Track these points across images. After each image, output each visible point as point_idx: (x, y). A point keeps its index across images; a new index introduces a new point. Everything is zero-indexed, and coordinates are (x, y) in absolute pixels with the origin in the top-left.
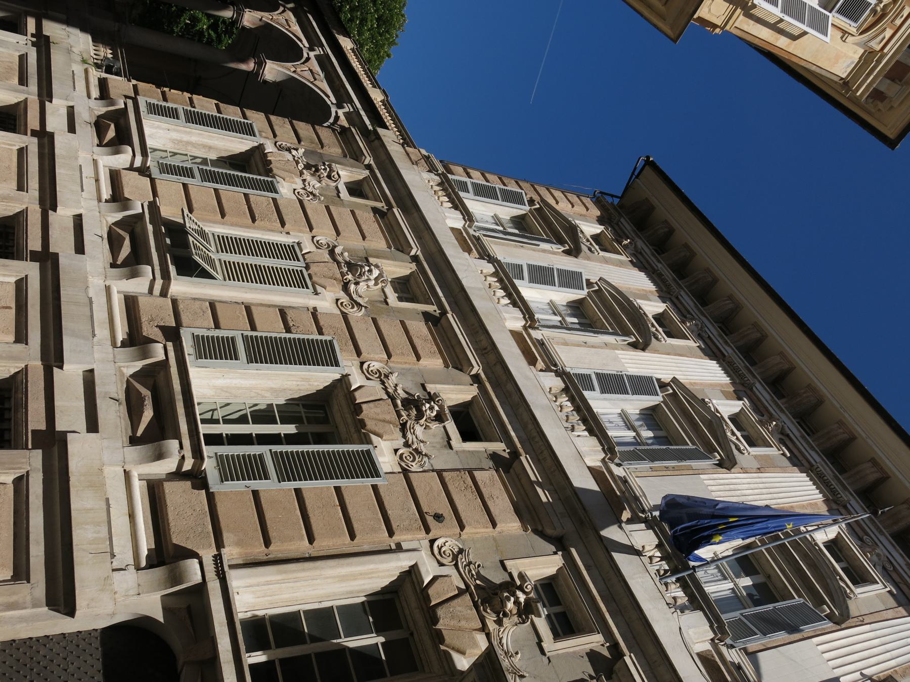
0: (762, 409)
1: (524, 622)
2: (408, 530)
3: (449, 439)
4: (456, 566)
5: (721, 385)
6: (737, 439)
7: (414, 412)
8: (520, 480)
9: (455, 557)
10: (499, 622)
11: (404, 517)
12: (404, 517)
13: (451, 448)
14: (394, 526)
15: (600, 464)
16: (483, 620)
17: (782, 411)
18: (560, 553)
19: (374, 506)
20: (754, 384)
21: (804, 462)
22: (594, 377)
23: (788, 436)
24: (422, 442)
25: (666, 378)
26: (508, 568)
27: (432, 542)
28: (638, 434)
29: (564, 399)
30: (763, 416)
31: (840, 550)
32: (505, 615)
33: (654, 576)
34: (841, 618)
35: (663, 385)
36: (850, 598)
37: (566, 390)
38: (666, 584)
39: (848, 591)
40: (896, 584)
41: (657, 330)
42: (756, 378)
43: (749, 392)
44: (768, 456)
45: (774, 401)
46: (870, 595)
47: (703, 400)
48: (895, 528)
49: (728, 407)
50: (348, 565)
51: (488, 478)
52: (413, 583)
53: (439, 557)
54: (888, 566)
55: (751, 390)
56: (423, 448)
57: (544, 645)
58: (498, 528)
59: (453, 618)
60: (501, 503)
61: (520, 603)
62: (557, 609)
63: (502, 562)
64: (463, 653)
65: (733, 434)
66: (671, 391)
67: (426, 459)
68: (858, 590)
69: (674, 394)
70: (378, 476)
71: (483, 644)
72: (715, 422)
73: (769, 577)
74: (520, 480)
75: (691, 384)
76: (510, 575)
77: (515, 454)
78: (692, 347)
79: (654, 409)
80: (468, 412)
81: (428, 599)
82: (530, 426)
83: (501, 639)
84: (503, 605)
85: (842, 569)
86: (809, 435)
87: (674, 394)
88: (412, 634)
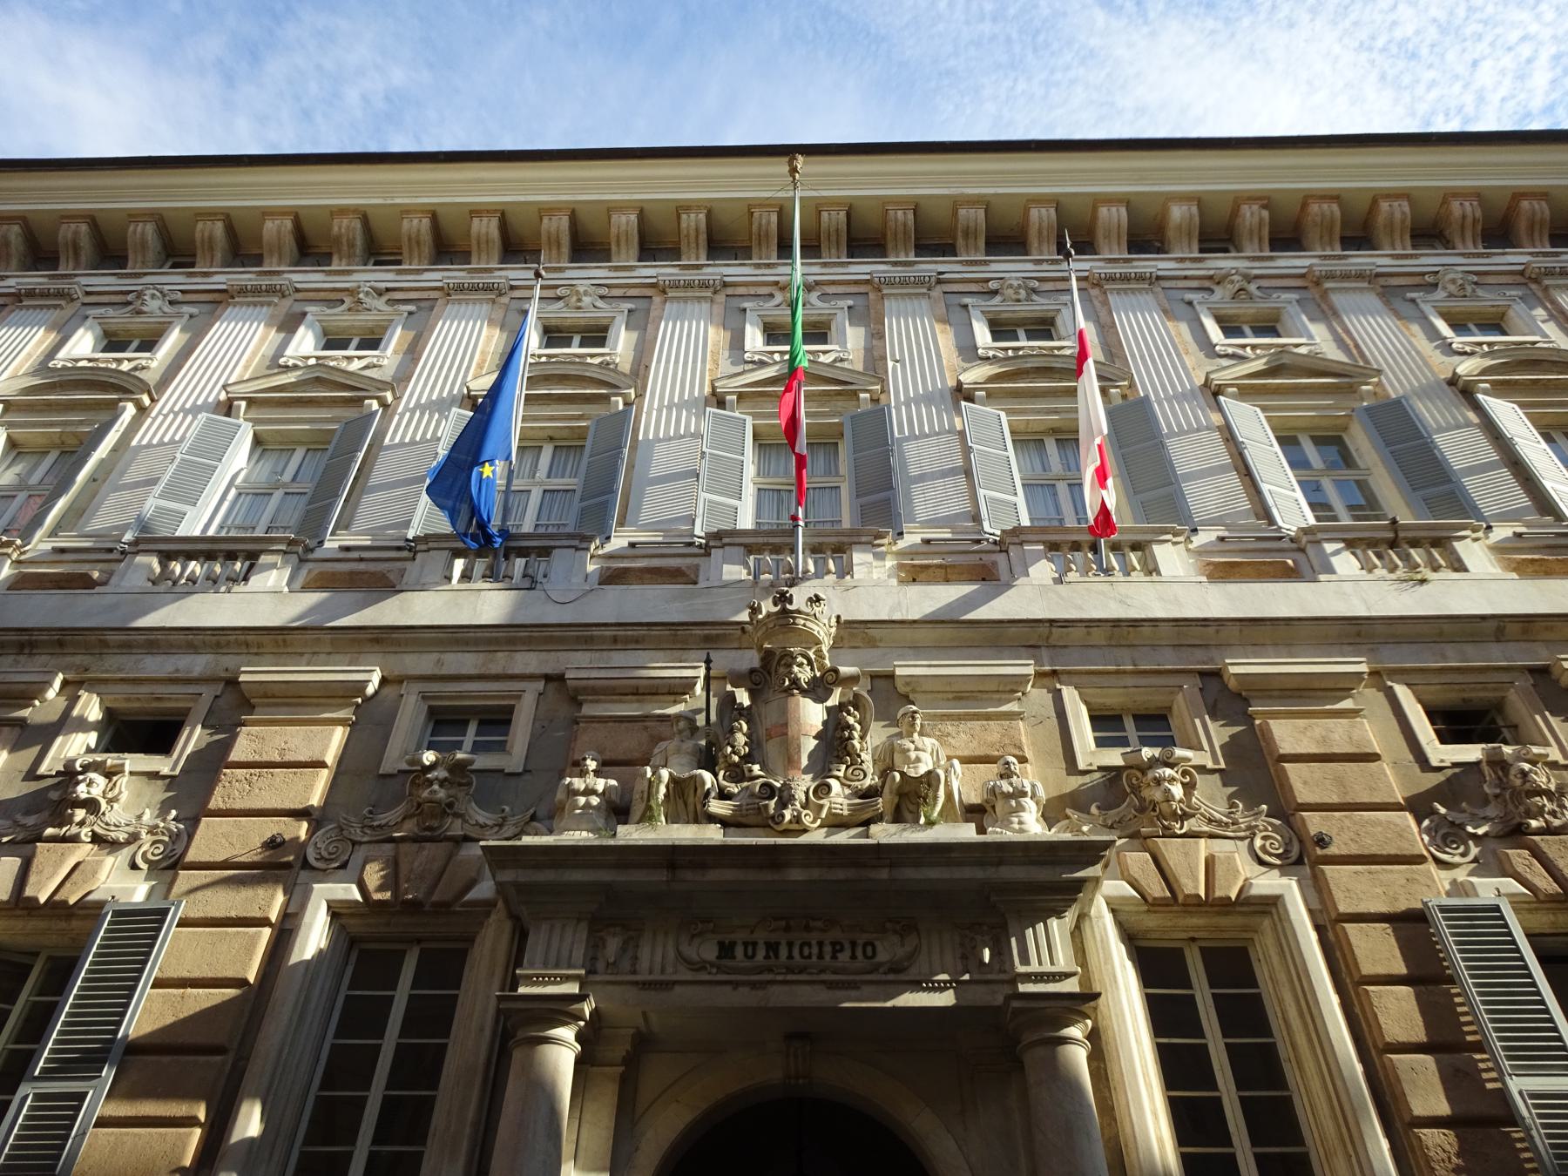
6: (359, 358)
7: (80, 814)
8: (274, 697)
14: (258, 914)
23: (388, 290)
26: (391, 771)
27: (306, 865)
30: (343, 302)
32: (450, 805)
33: (488, 585)
35: (228, 408)
37: (166, 557)
41: (129, 360)
43: (299, 296)
55: (297, 290)
61: (446, 779)
64: (471, 884)
65: (349, 359)
69: (251, 402)
70: (165, 912)
72: (320, 377)
73: (551, 438)
79: (258, 441)
80: (123, 722)
83: (477, 824)
85: (581, 345)
86: (399, 263)
87: (251, 402)
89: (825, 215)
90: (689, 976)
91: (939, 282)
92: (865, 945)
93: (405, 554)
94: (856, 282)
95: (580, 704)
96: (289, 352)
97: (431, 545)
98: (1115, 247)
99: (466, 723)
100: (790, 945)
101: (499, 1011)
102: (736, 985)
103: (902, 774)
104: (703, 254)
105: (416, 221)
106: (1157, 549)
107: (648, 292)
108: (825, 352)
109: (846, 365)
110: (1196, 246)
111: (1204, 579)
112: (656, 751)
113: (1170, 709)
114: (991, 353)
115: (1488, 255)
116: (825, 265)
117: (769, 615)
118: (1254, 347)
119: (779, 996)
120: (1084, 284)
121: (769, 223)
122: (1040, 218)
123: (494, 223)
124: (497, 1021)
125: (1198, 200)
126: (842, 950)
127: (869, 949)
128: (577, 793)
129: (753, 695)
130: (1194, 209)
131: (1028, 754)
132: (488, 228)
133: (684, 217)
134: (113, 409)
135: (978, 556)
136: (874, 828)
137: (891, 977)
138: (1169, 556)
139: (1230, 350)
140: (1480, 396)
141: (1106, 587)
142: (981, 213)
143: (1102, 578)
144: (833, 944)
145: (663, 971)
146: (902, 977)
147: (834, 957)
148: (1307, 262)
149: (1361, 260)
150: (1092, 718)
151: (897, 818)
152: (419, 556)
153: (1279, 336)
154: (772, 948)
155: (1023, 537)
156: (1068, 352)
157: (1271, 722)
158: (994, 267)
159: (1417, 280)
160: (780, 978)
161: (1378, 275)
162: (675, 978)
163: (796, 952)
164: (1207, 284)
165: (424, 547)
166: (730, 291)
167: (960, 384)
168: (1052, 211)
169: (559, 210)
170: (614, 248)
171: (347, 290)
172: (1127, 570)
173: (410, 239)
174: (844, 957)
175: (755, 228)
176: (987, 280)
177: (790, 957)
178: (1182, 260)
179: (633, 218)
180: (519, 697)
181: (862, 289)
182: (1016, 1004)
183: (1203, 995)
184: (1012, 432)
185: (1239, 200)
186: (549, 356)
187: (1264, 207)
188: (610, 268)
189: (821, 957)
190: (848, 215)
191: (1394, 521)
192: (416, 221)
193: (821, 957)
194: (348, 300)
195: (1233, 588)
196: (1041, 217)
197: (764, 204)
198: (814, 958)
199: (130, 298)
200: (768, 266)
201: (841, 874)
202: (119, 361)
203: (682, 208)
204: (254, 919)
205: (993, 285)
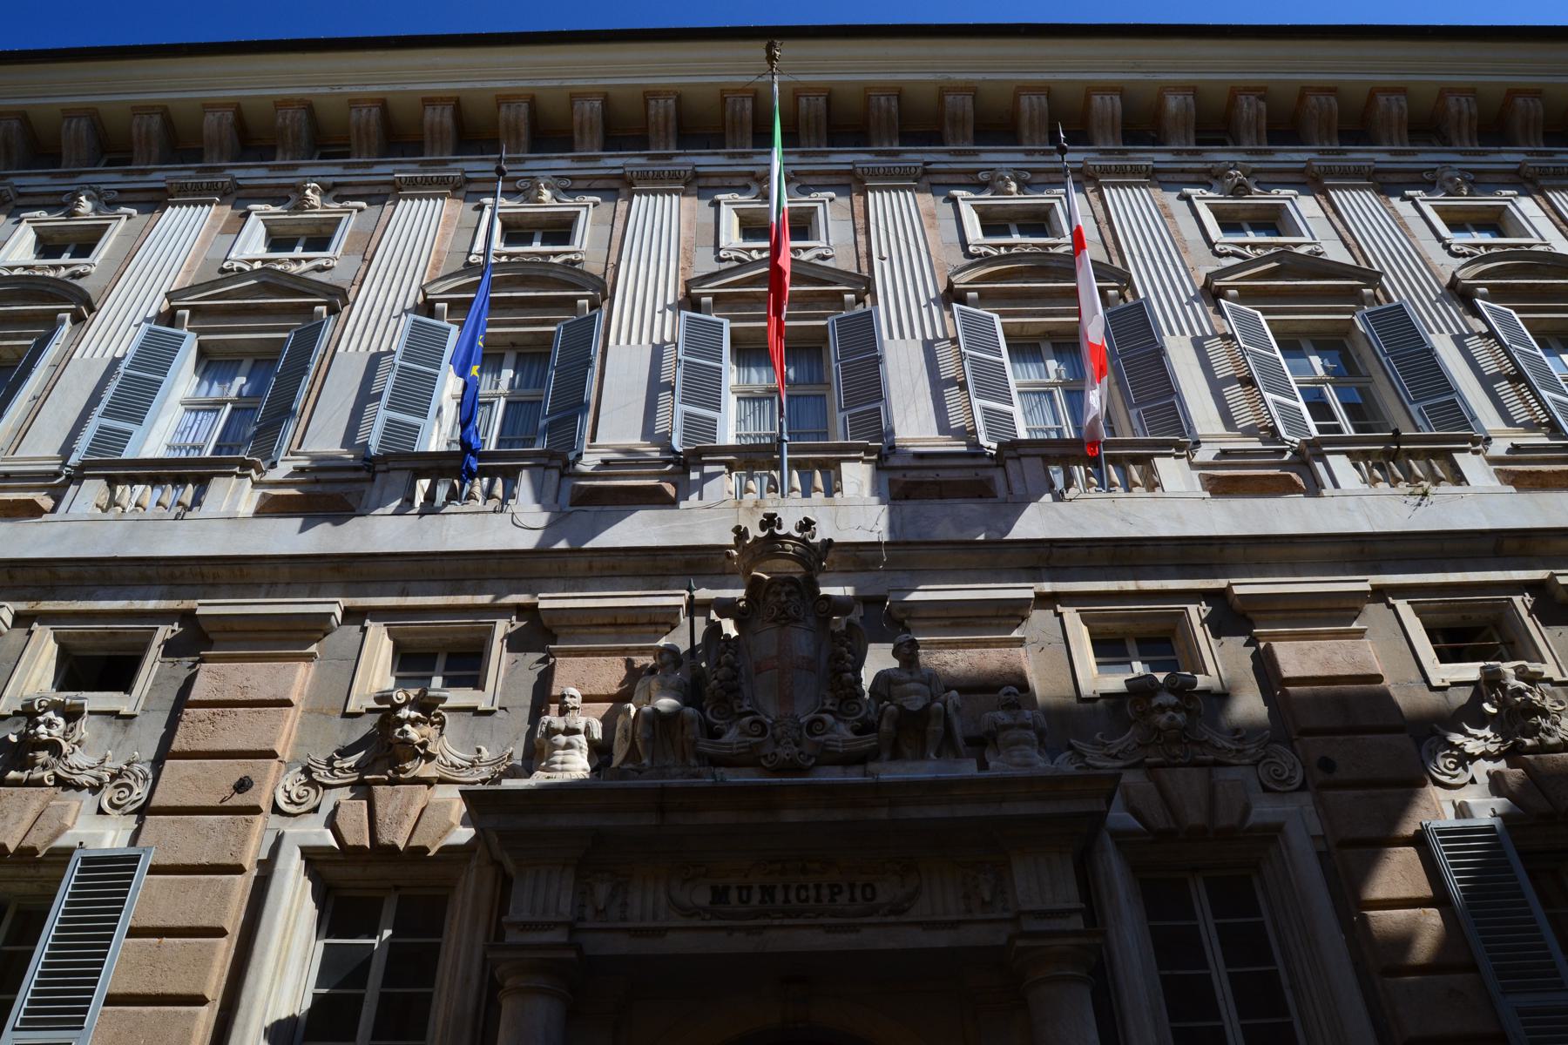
0: (277, 193)
1: (442, 723)
2: (243, 841)
3: (115, 714)
4: (326, 787)
5: (212, 227)
6: (307, 260)
7: (43, 756)
8: (232, 631)
9: (312, 783)
10: (430, 757)
11: (221, 840)
12: (221, 840)
13: (132, 717)
14: (229, 861)
15: (258, 492)
16: (417, 781)
17: (295, 167)
18: (368, 622)
19: (183, 881)
20: (233, 179)
21: (384, 190)
22: (108, 422)
23: (335, 185)
24: (103, 761)
25: (160, 304)
26: (358, 710)
27: (276, 809)
28: (232, 402)
29: (129, 495)
31: (519, 227)
32: (424, 745)
34: (602, 290)
35: (169, 318)
36: (581, 261)
37: (112, 482)
39: (572, 257)
40: (589, 191)
41: (67, 266)
42: (225, 168)
43: (242, 193)
44: (352, 233)
45: (273, 168)
46: (591, 227)
47: (222, 271)
48: (524, 139)
49: (252, 245)
50: (264, 954)
51: (211, 680)
52: (327, 861)
53: (304, 808)
54: (564, 183)
55: (240, 187)
56: (112, 765)
57: (482, 707)
58: (294, 699)
59: (399, 823)
60: (255, 678)
62: (441, 662)
63: (346, 715)
65: (297, 261)
66: (187, 312)
67: (136, 768)
68: (575, 247)
69: (196, 311)
70: (136, 859)
71: (451, 794)
72: (270, 281)
74: (232, 631)
75: (188, 272)
76: (370, 711)
77: (187, 617)
78: (126, 229)
79: (203, 352)
80: (77, 658)
81: (359, 849)
82: (151, 571)
83: (453, 765)
84: (408, 742)
87: (196, 311)
88: (397, 888)
89: (803, 101)
90: (681, 922)
91: (926, 172)
92: (864, 886)
93: (363, 474)
94: (838, 173)
96: (233, 255)
97: (391, 464)
98: (1110, 137)
99: (435, 655)
100: (786, 888)
101: (485, 960)
102: (731, 930)
103: (901, 708)
104: (672, 143)
105: (365, 111)
106: (1159, 462)
107: (615, 184)
108: (806, 249)
109: (829, 263)
110: (1192, 138)
111: (1207, 494)
112: (639, 686)
113: (1173, 631)
114: (983, 250)
115: (1485, 153)
116: (803, 154)
117: (756, 539)
118: (1254, 246)
119: (780, 940)
120: (1078, 177)
121: (743, 108)
122: (1031, 105)
123: (448, 112)
124: (483, 969)
125: (1193, 89)
126: (840, 892)
127: (868, 890)
128: (557, 732)
129: (738, 626)
130: (1190, 99)
132: (442, 117)
133: (653, 103)
134: (52, 323)
135: (973, 472)
136: (872, 766)
137: (892, 919)
138: (1169, 469)
139: (1230, 249)
140: (1479, 302)
141: (1107, 504)
142: (969, 101)
143: (1104, 494)
144: (831, 886)
145: (655, 918)
146: (903, 919)
147: (832, 900)
148: (1305, 156)
149: (1360, 156)
150: (1094, 643)
151: (896, 755)
152: (379, 477)
153: (1280, 235)
154: (768, 891)
155: (1021, 451)
156: (1061, 250)
157: (1274, 644)
158: (983, 157)
159: (1416, 177)
160: (777, 922)
161: (1377, 171)
162: (665, 924)
163: (792, 896)
164: (1205, 178)
165: (384, 467)
166: (702, 182)
167: (950, 284)
168: (1044, 99)
169: (519, 96)
170: (577, 136)
171: (292, 186)
172: (1128, 485)
173: (358, 130)
174: (843, 899)
175: (728, 114)
176: (977, 171)
177: (787, 901)
178: (1178, 152)
179: (597, 104)
181: (844, 180)
182: (1020, 943)
183: (1207, 926)
184: (1007, 336)
185: (1236, 92)
186: (510, 255)
187: (1261, 98)
188: (573, 159)
189: (818, 900)
190: (828, 101)
191: (1396, 432)
192: (365, 111)
193: (818, 900)
194: (293, 197)
195: (1238, 504)
196: (1031, 105)
197: (741, 91)
198: (812, 902)
199: (64, 199)
200: (743, 155)
201: (839, 815)
202: (56, 268)
203: (649, 95)
204: (228, 866)
205: (983, 177)
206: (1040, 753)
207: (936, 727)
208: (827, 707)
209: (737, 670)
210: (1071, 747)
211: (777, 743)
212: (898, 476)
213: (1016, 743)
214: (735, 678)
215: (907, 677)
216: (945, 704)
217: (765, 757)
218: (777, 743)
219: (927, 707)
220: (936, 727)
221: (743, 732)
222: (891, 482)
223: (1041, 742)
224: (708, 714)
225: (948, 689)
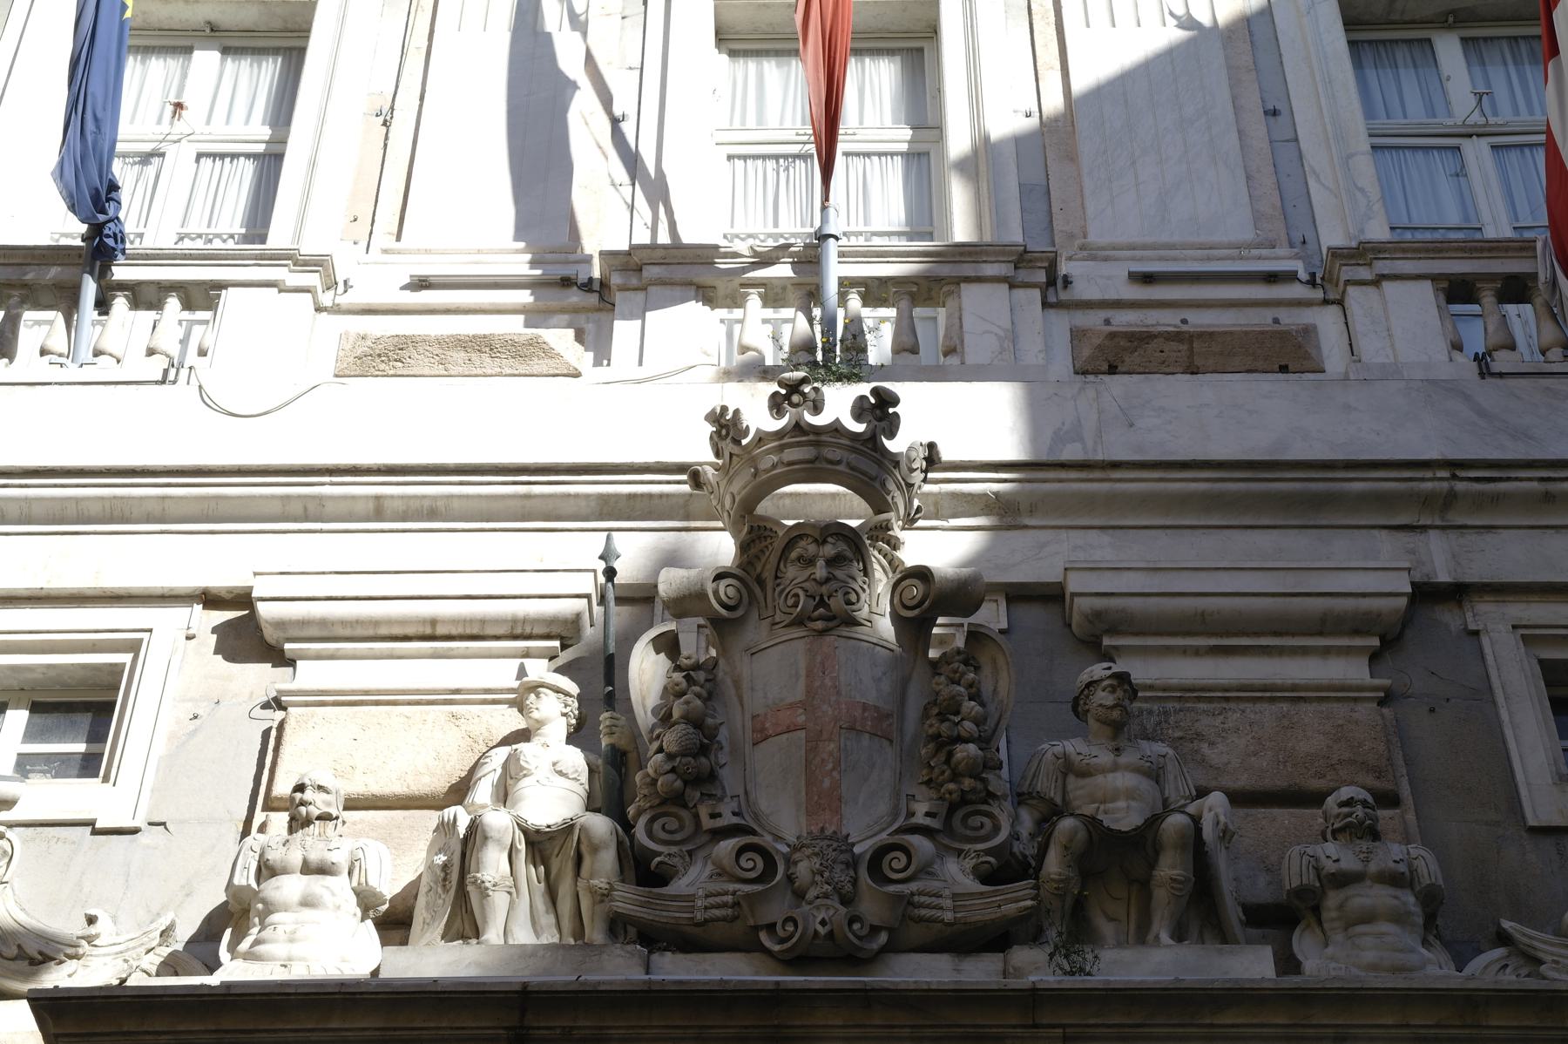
38: (98, 353)
95: (291, 663)
103: (1092, 823)
131: (1405, 791)
136: (1022, 956)
155: (1383, 267)
180: (134, 647)
206: (1425, 943)
207: (1171, 868)
208: (919, 819)
209: (712, 735)
210: (1503, 939)
211: (800, 895)
212: (1093, 320)
213: (1368, 917)
214: (704, 750)
215: (1105, 758)
216: (1196, 820)
217: (771, 928)
218: (800, 895)
219: (1154, 821)
220: (1171, 868)
221: (721, 873)
222: (1077, 335)
223: (1430, 920)
224: (640, 832)
225: (1202, 793)
